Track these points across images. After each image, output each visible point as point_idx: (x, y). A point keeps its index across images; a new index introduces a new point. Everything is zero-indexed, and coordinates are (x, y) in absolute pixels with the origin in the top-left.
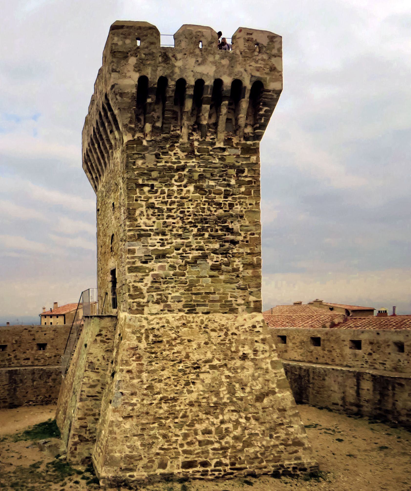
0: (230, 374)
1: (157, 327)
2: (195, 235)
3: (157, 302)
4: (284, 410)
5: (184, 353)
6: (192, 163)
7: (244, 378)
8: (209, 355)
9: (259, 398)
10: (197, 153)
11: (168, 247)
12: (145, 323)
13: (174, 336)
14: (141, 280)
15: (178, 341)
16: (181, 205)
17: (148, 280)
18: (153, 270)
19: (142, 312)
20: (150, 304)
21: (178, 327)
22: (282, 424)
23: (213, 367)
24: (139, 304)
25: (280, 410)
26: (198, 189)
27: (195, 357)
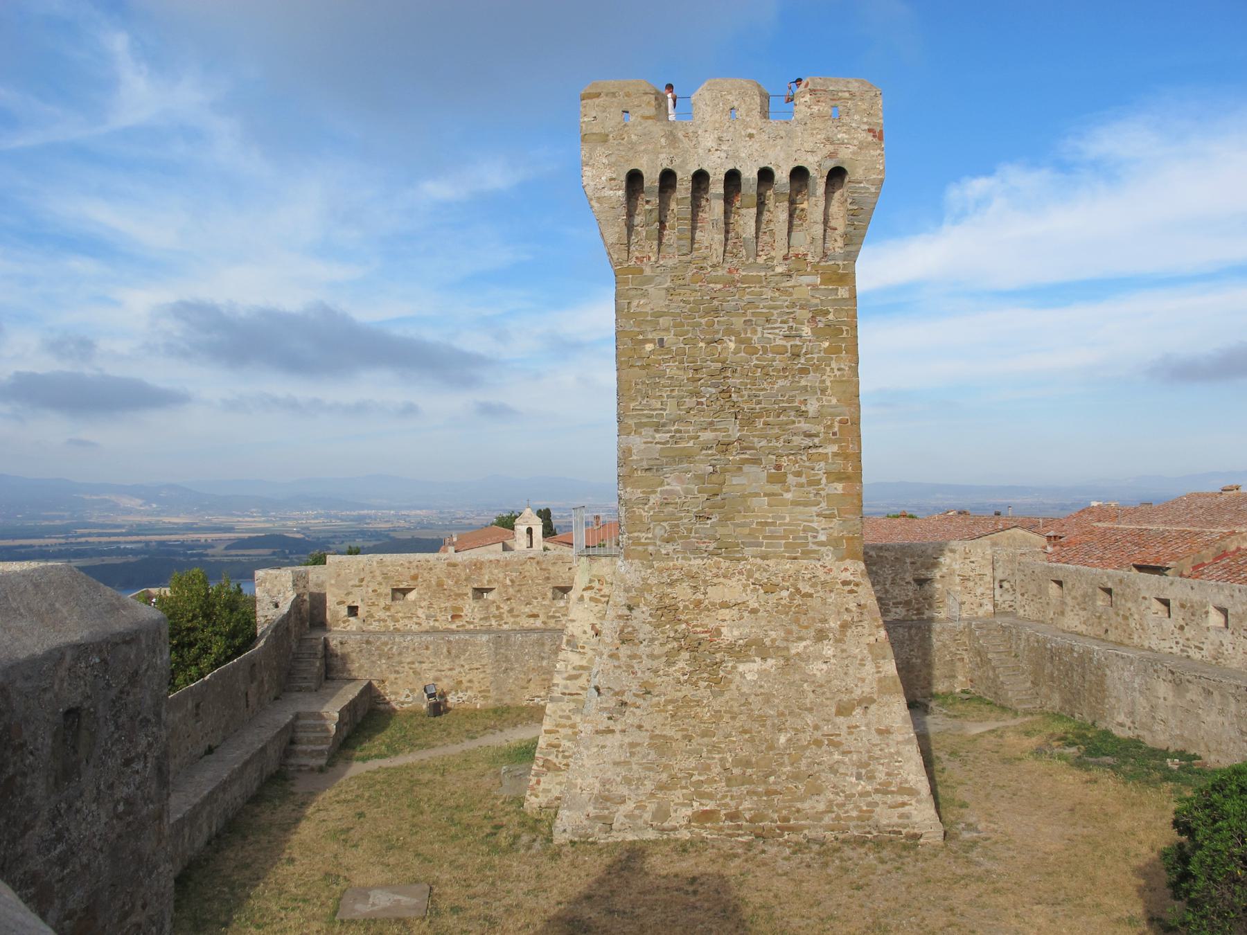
7: (819, 674)
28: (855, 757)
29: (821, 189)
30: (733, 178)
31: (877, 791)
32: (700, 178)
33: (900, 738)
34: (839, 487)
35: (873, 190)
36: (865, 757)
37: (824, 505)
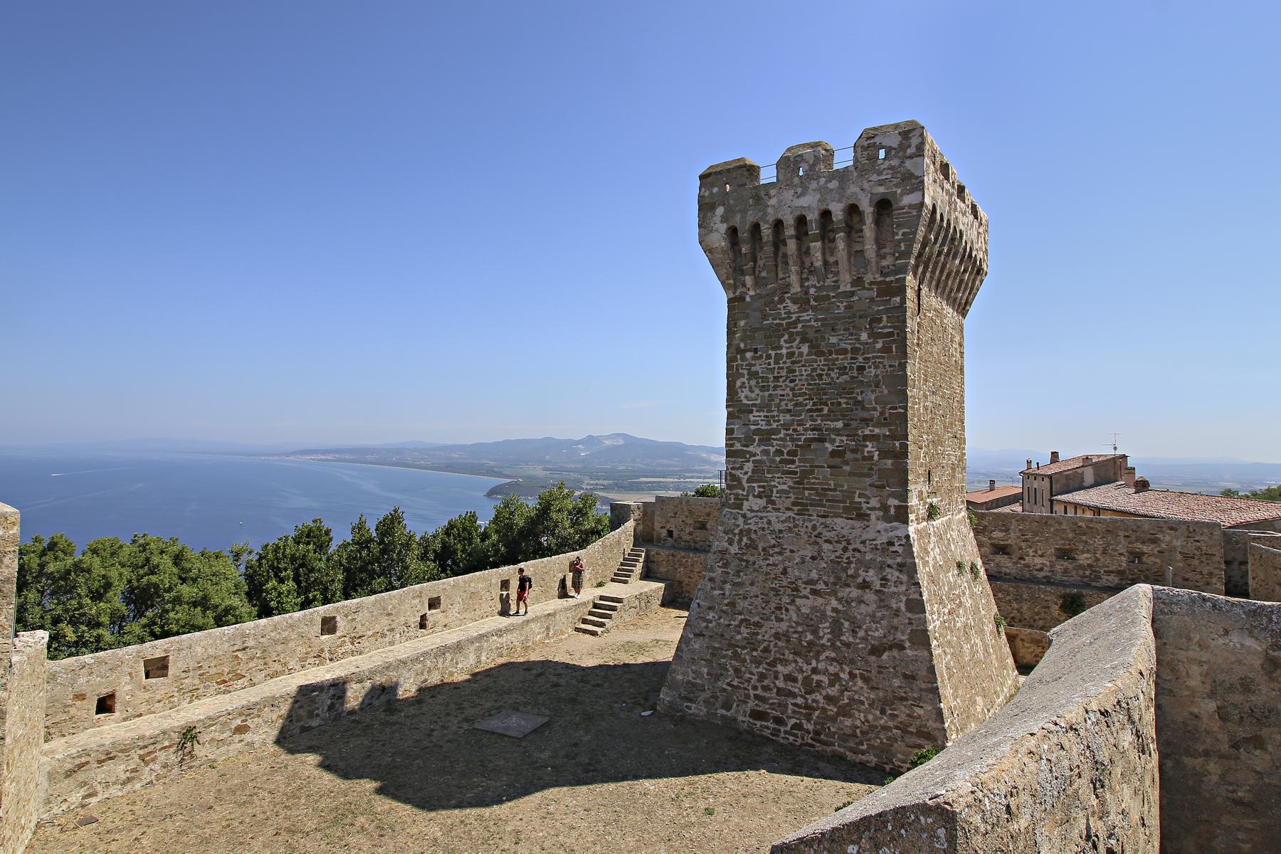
0: (840, 607)
1: (754, 528)
2: (808, 411)
3: (759, 496)
4: (913, 678)
5: (781, 567)
6: (805, 316)
8: (814, 575)
9: (876, 651)
10: (813, 303)
11: (774, 426)
12: (741, 521)
13: (773, 542)
14: (741, 468)
15: (777, 550)
16: (791, 371)
17: (749, 466)
18: (755, 455)
19: (740, 507)
20: (751, 498)
21: (780, 531)
22: (906, 699)
23: (815, 592)
24: (737, 497)
25: (905, 676)
26: (816, 349)
27: (794, 573)
28: (881, 694)
29: (869, 220)
30: (801, 221)
31: (897, 728)
32: (778, 224)
33: (924, 686)
34: (889, 463)
35: (915, 213)
36: (890, 696)
37: (875, 477)
